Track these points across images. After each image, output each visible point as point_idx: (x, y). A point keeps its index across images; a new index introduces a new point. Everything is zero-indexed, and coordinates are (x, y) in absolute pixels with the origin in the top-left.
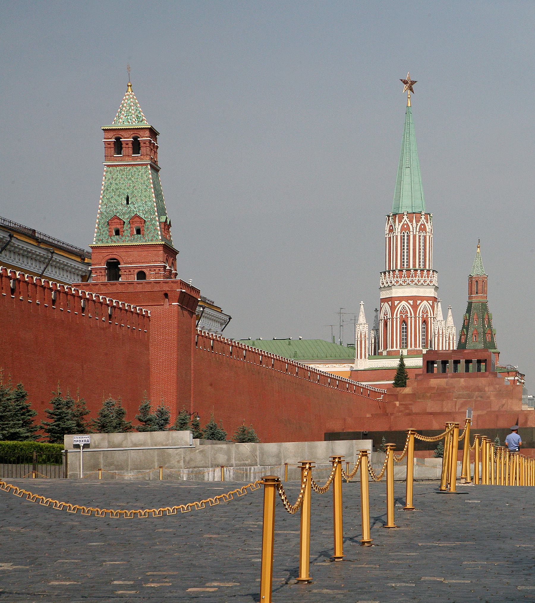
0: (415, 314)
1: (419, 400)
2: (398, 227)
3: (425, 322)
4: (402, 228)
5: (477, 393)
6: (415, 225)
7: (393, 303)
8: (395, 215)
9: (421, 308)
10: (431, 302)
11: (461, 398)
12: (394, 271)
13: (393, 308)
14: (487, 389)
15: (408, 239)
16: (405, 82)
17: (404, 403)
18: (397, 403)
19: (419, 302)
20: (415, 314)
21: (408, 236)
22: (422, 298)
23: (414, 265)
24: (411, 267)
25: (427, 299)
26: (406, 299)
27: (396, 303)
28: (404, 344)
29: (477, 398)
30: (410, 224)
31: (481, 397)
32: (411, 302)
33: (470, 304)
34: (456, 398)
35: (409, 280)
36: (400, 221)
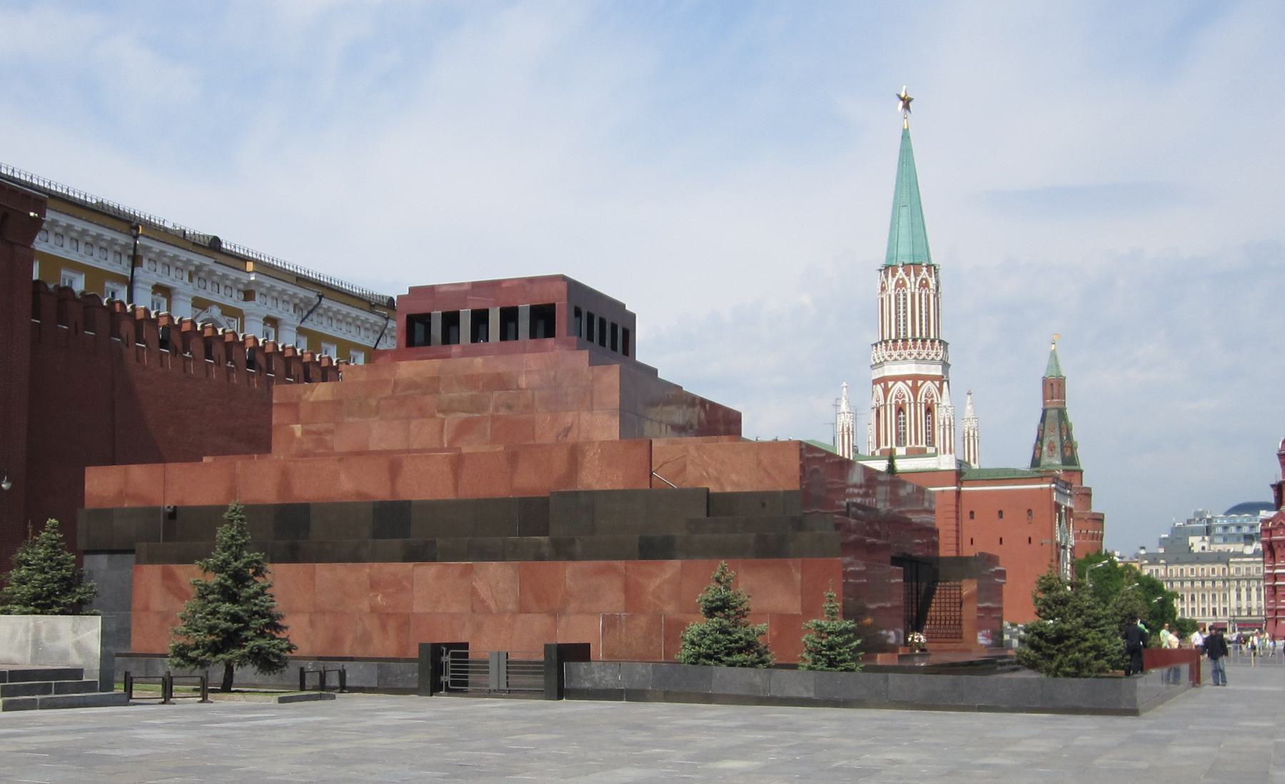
0: (915, 399)
1: (350, 419)
2: (891, 283)
3: (929, 410)
4: (897, 285)
5: (496, 394)
6: (913, 279)
7: (886, 385)
8: (887, 268)
9: (923, 391)
10: (937, 383)
11: (455, 411)
12: (886, 342)
13: (886, 391)
14: (523, 382)
15: (905, 299)
16: (903, 99)
17: (313, 427)
18: (298, 429)
19: (920, 383)
20: (915, 399)
21: (905, 295)
22: (925, 378)
23: (914, 333)
24: (909, 335)
25: (932, 378)
26: (903, 378)
27: (890, 384)
28: (900, 440)
29: (497, 409)
30: (906, 279)
31: (510, 407)
32: (910, 383)
33: (1045, 411)
34: (443, 412)
35: (905, 353)
36: (894, 276)
